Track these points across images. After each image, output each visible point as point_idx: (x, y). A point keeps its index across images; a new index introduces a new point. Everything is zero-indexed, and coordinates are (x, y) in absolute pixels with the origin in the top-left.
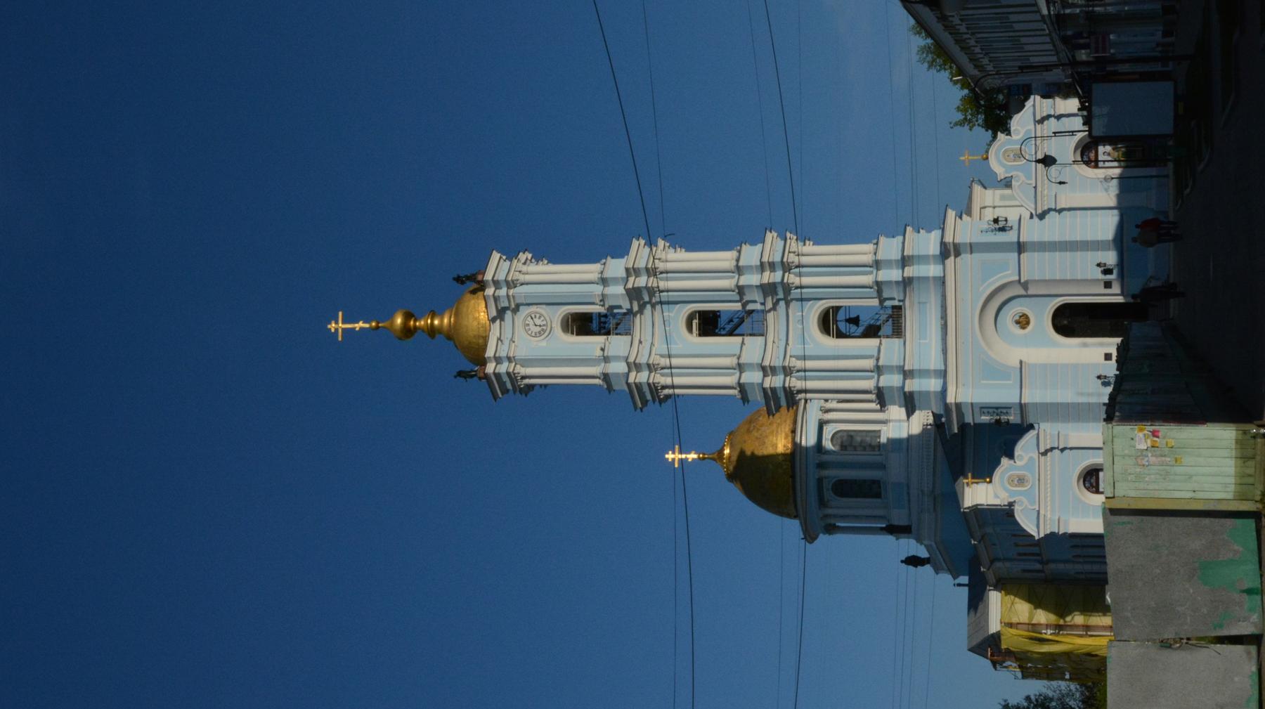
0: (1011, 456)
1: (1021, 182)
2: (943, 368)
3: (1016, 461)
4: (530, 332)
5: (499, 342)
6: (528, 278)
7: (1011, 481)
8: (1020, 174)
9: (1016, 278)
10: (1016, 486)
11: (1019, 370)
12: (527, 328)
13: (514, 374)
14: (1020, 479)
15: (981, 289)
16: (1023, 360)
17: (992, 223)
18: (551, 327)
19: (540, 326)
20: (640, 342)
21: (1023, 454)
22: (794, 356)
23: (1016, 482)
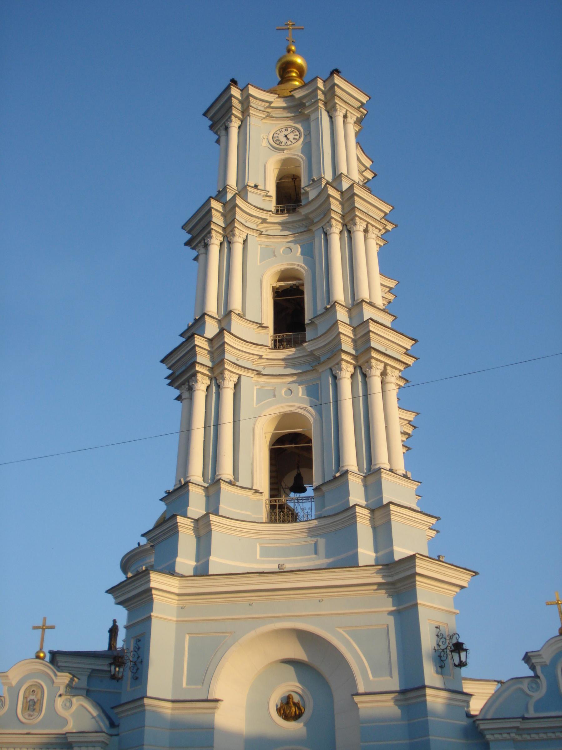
0: (72, 689)
1: (530, 693)
2: (210, 573)
3: (63, 698)
4: (278, 132)
5: (267, 104)
6: (340, 120)
7: (36, 689)
8: (544, 690)
9: (361, 689)
10: (25, 698)
11: (204, 697)
12: (283, 130)
13: (230, 117)
14: (35, 703)
15: (341, 631)
16: (221, 705)
17: (454, 641)
18: (283, 150)
19: (288, 139)
20: (264, 221)
21: (74, 708)
22: (239, 378)
23: (32, 697)
